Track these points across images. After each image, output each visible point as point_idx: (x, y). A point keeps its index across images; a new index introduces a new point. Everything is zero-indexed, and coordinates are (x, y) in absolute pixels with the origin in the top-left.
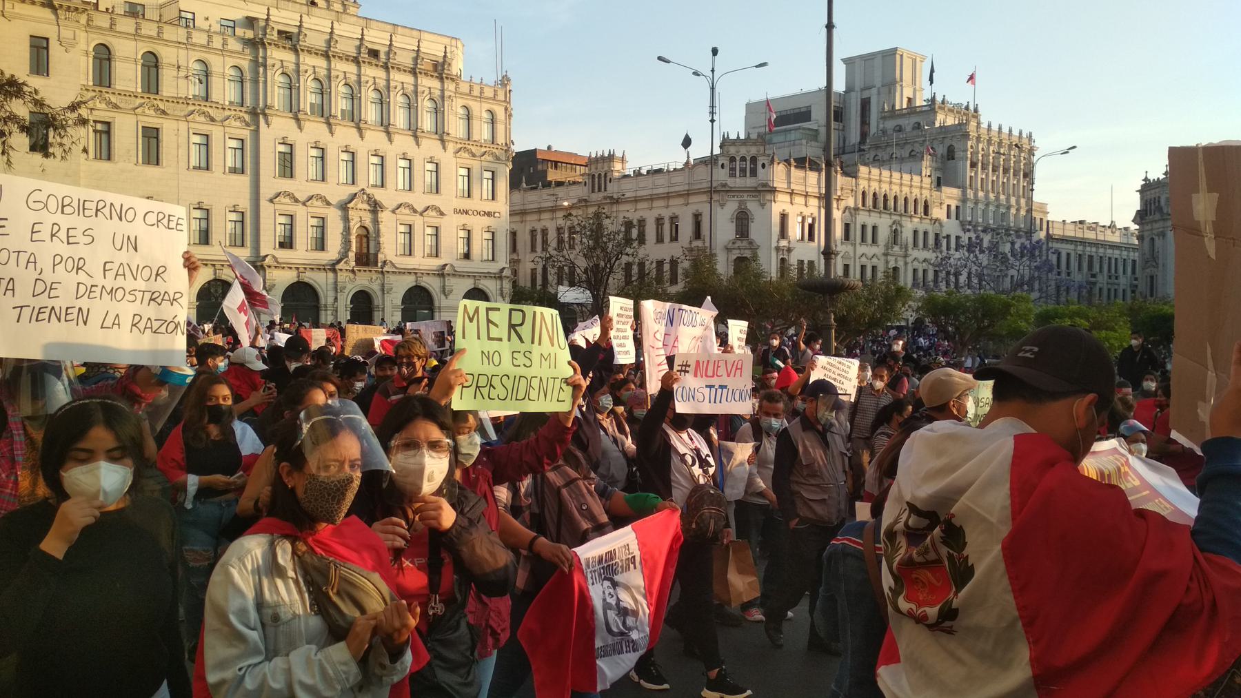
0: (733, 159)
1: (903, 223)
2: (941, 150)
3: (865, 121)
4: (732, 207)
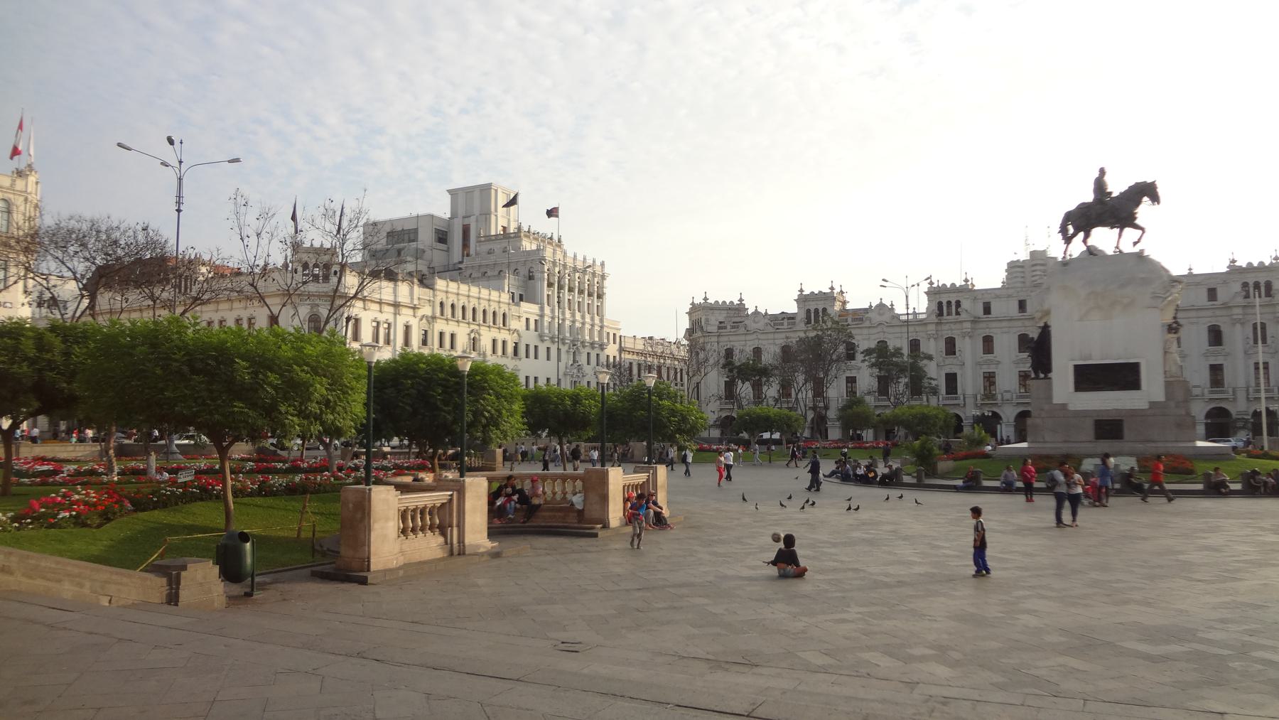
0: (305, 266)
1: (482, 332)
2: (523, 271)
3: (466, 244)
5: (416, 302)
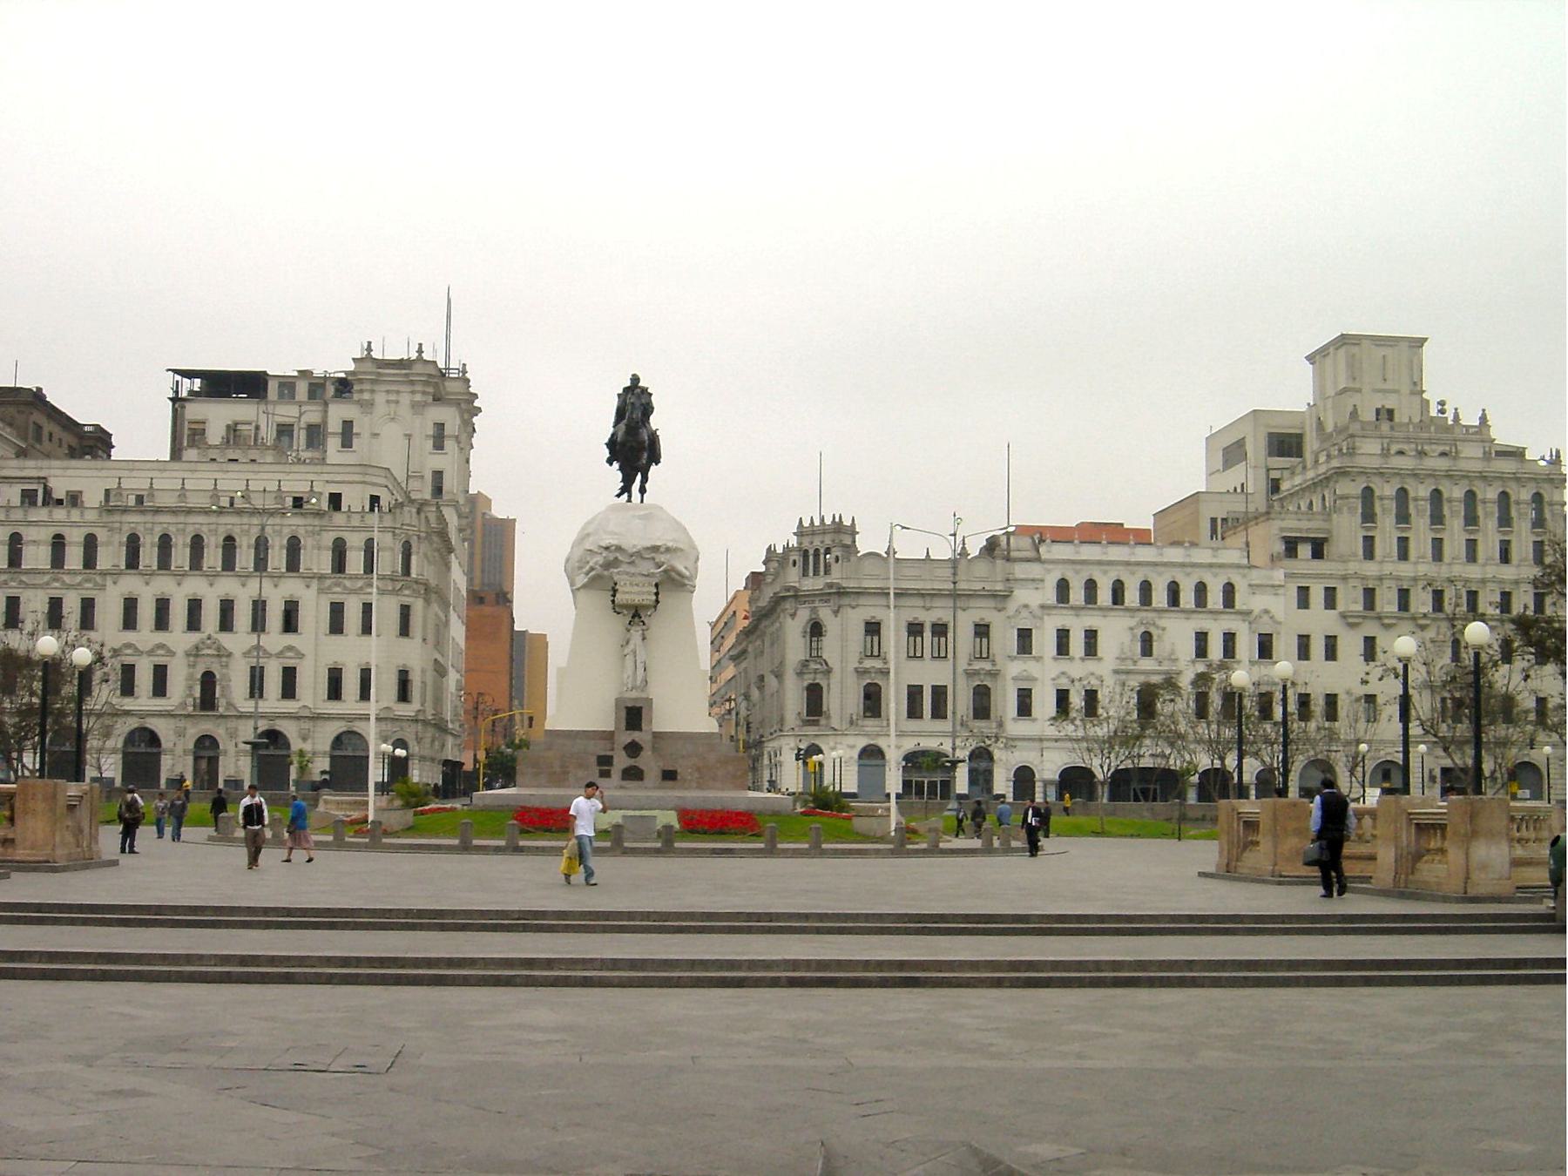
1: (1162, 623)
4: (804, 615)
5: (999, 587)
